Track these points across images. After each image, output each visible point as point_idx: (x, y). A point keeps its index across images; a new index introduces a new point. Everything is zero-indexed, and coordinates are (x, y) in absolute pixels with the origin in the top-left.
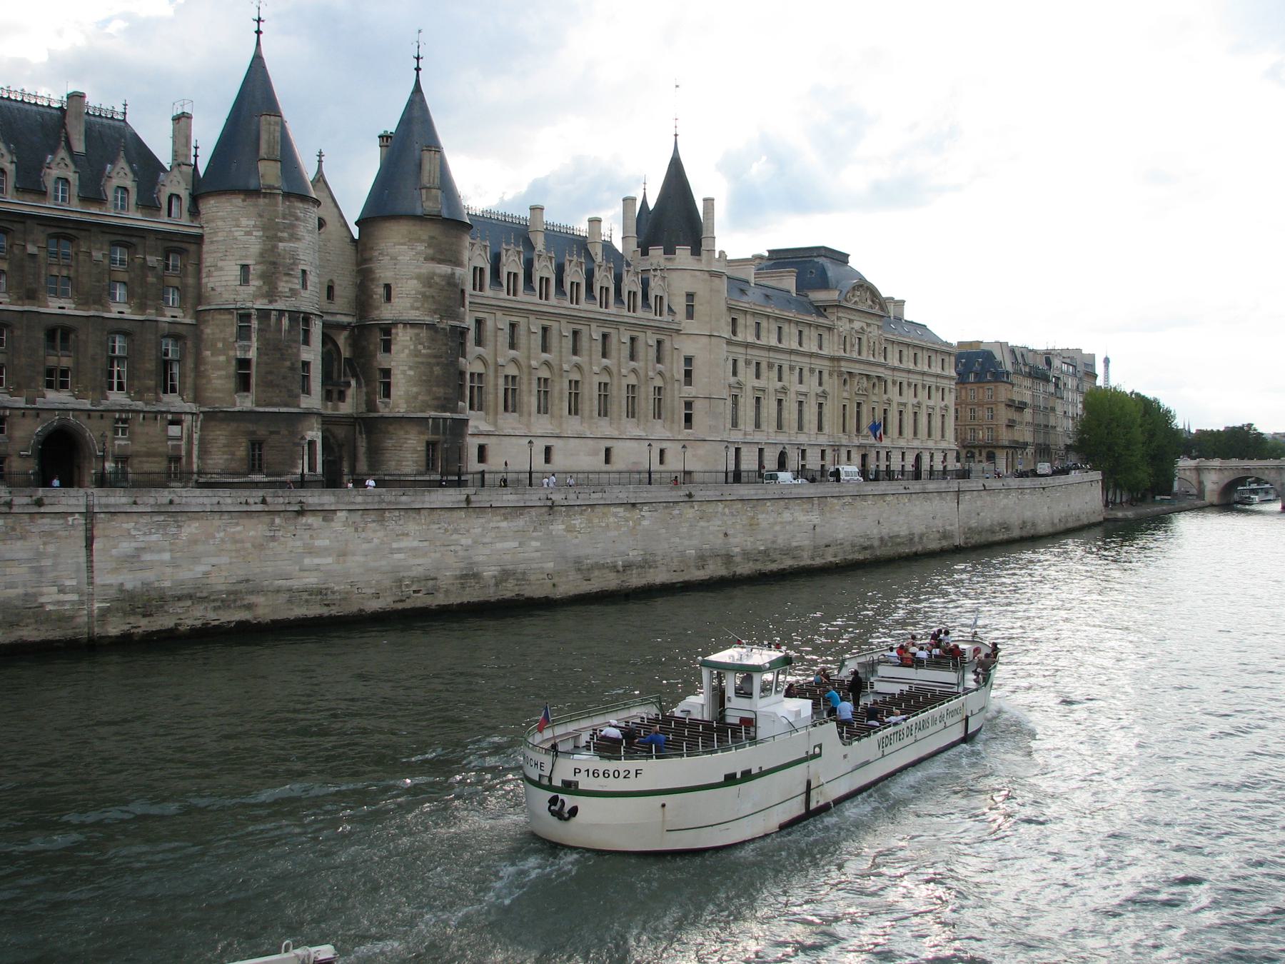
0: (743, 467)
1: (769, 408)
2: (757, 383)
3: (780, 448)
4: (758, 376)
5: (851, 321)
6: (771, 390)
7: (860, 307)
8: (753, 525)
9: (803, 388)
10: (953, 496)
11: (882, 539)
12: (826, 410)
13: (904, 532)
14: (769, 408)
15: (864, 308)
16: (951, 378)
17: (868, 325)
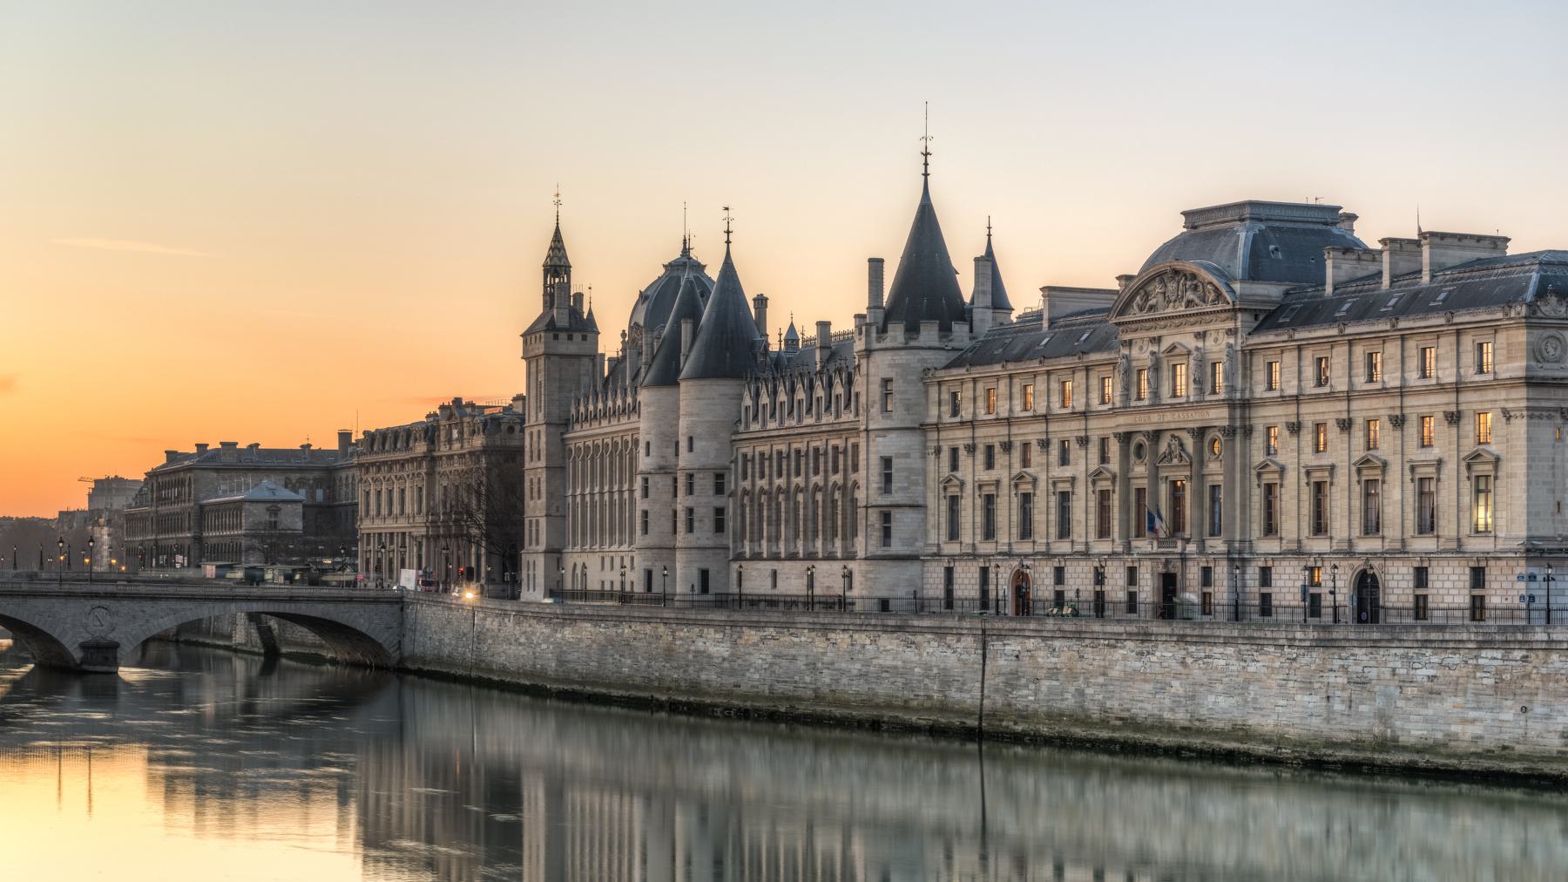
0: (958, 592)
1: (1007, 513)
2: (985, 476)
3: (1015, 563)
4: (990, 465)
5: (1157, 340)
6: (1005, 482)
7: (1170, 311)
8: (669, 653)
9: (1067, 472)
10: (968, 641)
11: (815, 690)
12: (1115, 500)
13: (861, 687)
14: (1007, 513)
15: (1181, 309)
16: (1511, 383)
17: (1201, 336)
